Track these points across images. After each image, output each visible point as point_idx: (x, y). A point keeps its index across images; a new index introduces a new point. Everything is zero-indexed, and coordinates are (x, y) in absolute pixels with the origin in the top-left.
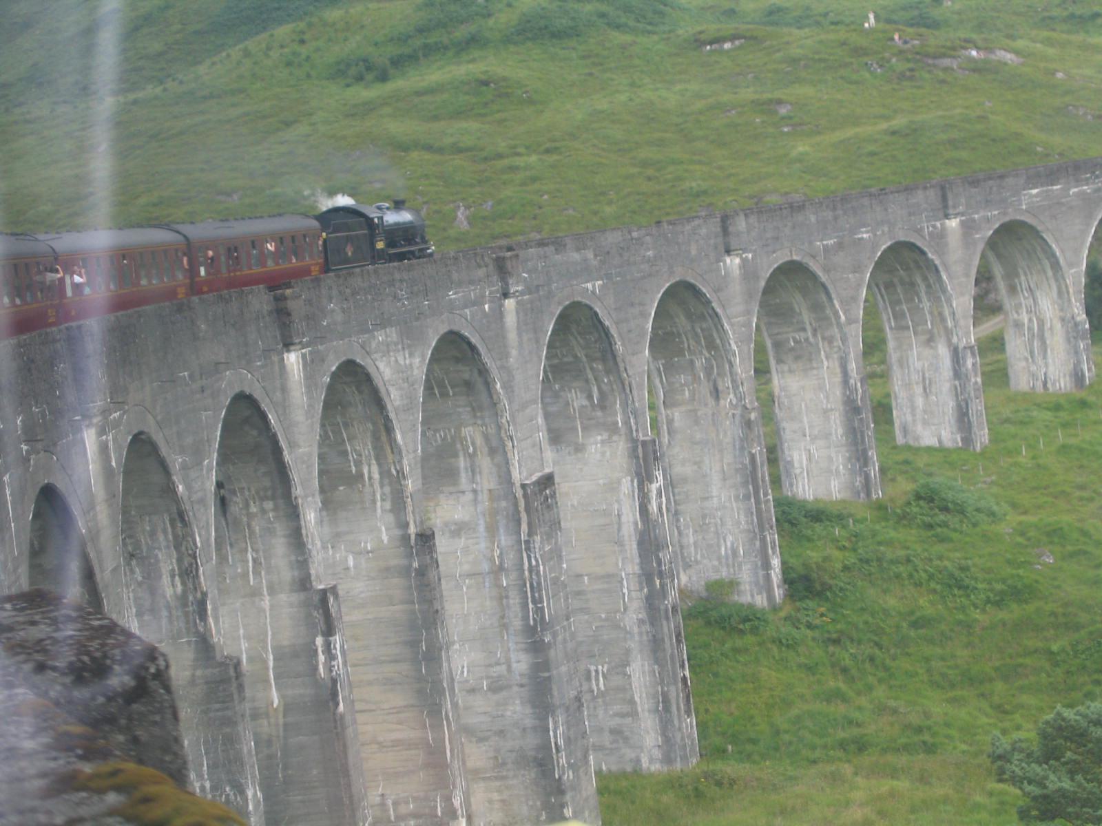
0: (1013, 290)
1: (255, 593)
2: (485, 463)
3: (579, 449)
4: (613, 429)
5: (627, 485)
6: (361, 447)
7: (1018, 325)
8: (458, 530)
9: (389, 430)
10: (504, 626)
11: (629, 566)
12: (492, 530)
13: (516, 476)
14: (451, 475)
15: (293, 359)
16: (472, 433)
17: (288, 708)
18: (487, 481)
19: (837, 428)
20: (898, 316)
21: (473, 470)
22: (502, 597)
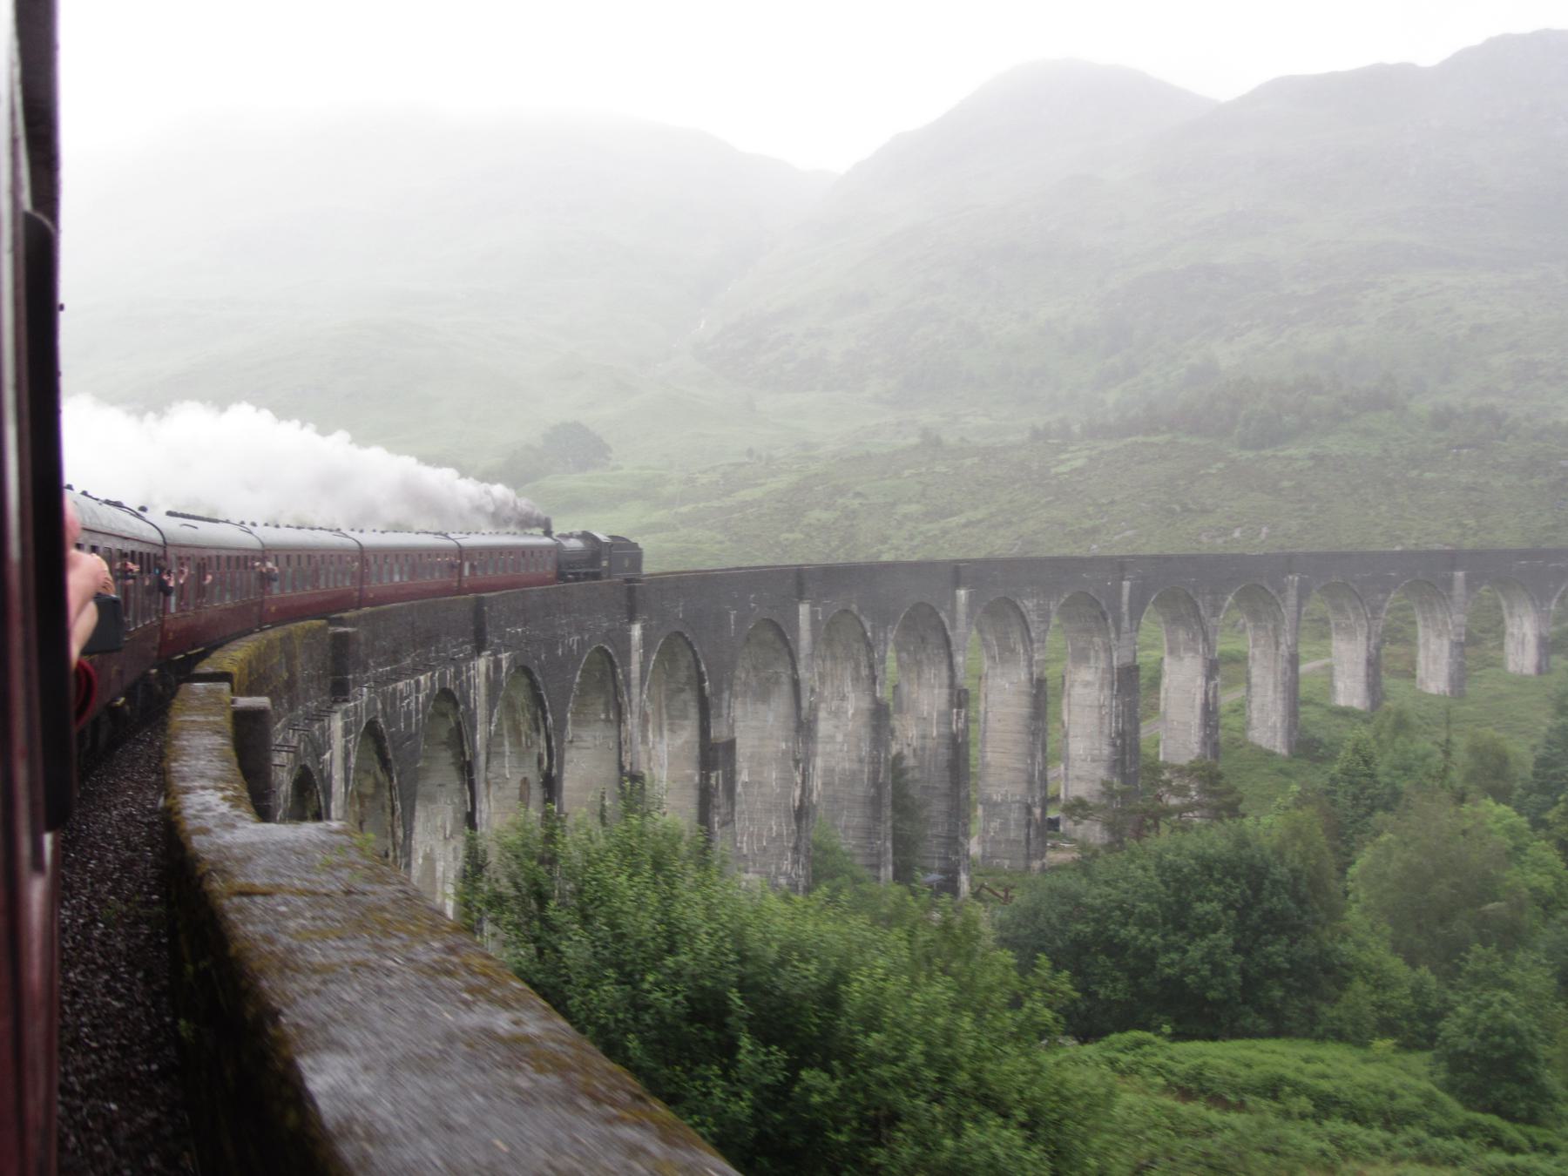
0: (1511, 615)
1: (933, 687)
2: (1102, 655)
3: (1181, 659)
4: (1196, 651)
5: (1200, 681)
6: (1016, 635)
7: (1512, 635)
8: (1087, 684)
9: (1028, 630)
10: (1101, 732)
11: (1195, 718)
12: (1102, 688)
13: (1115, 663)
14: (1087, 659)
15: (962, 593)
16: (1097, 640)
17: (939, 736)
18: (1102, 665)
19: (1361, 670)
20: (1425, 619)
21: (1097, 658)
22: (1101, 718)
